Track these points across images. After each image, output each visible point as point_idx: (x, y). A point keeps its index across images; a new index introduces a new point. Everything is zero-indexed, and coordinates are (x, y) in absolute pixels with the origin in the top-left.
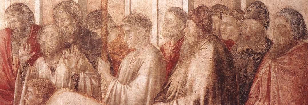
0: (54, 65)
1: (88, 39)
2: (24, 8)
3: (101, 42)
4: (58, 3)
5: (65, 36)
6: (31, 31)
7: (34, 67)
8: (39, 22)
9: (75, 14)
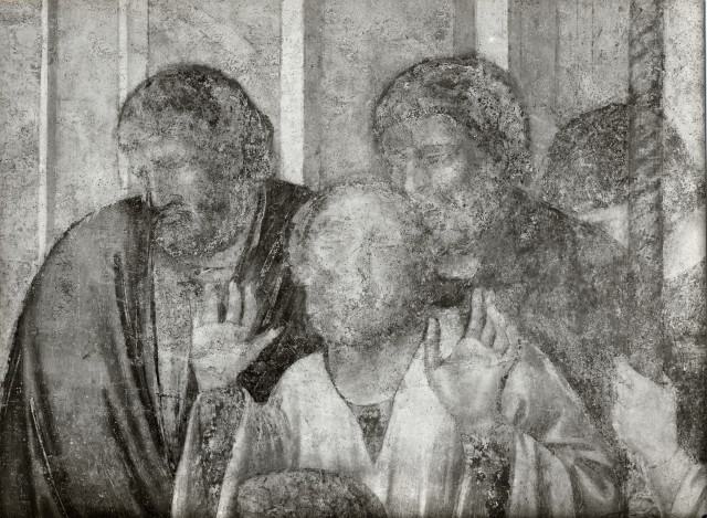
0: (380, 399)
1: (561, 258)
2: (220, 93)
3: (630, 276)
4: (399, 67)
5: (435, 241)
6: (256, 218)
7: (272, 412)
8: (299, 169)
9: (490, 129)
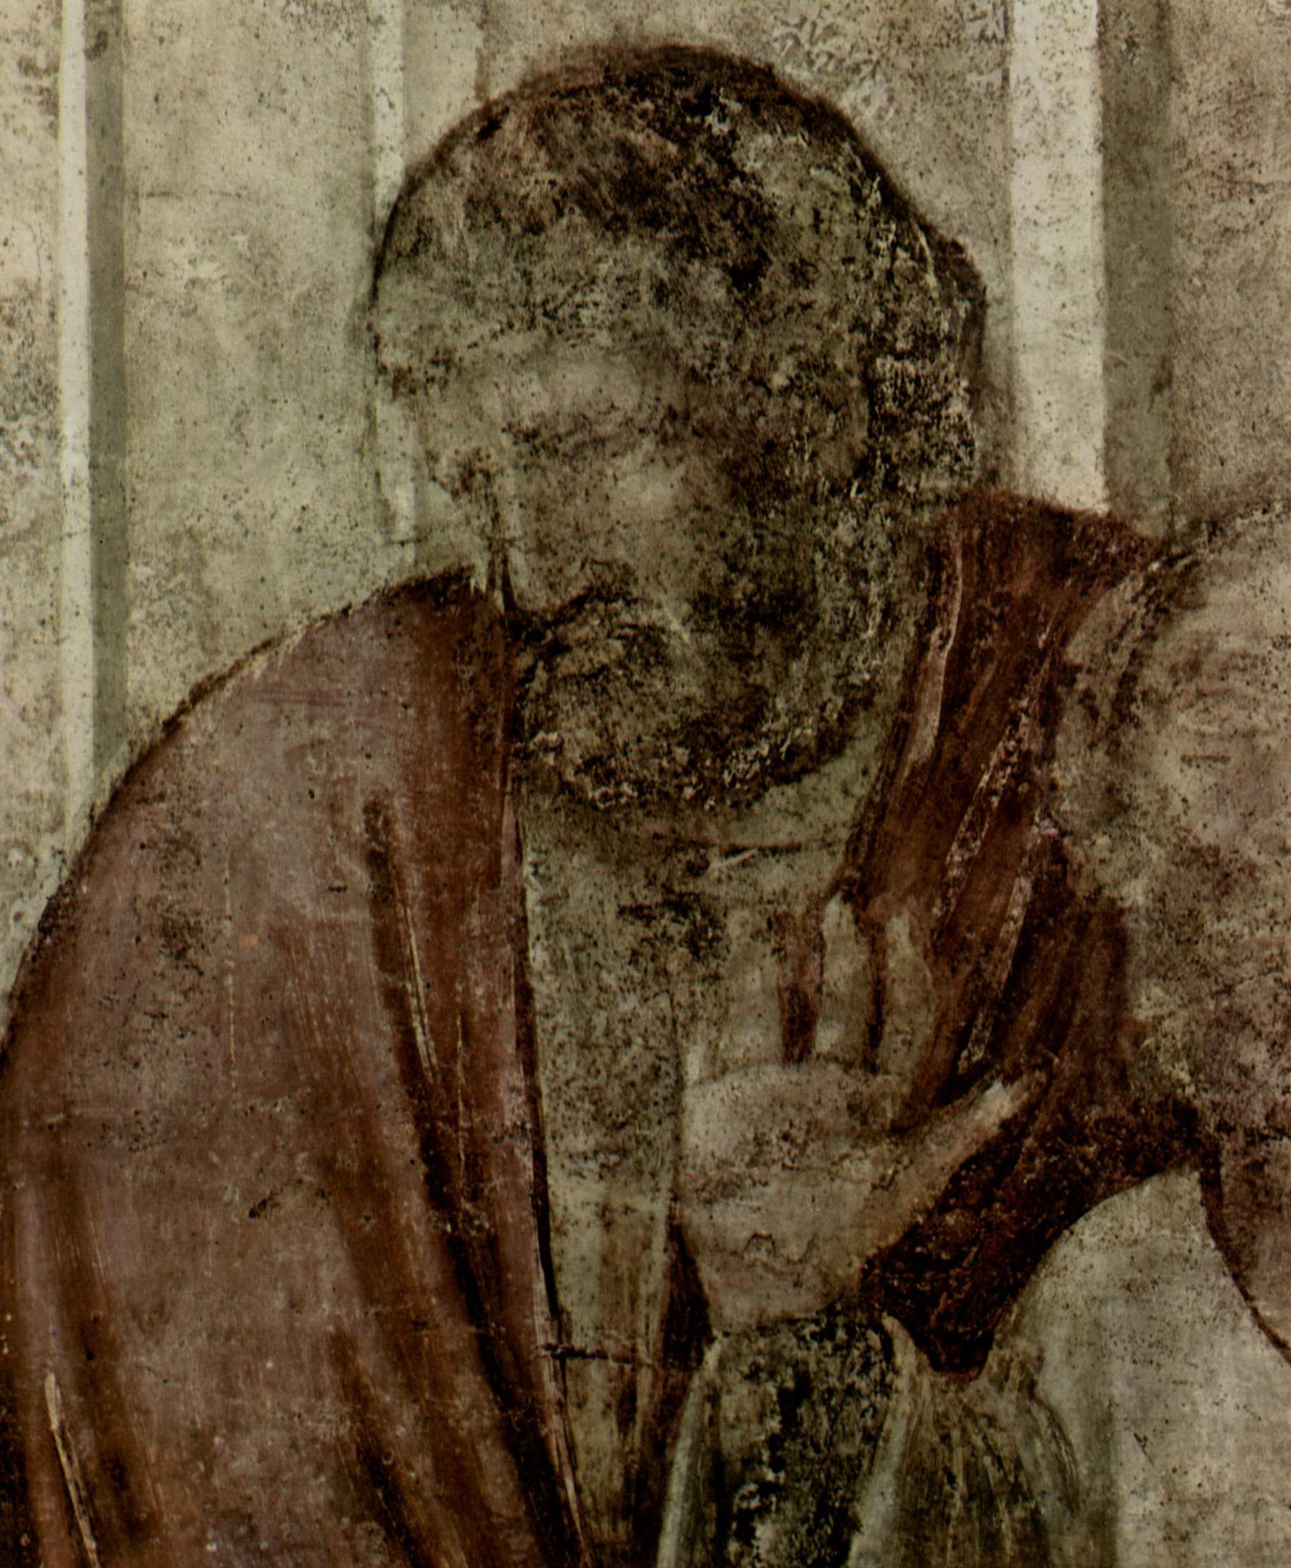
6: (922, 647)
7: (1005, 1405)
8: (1088, 451)
